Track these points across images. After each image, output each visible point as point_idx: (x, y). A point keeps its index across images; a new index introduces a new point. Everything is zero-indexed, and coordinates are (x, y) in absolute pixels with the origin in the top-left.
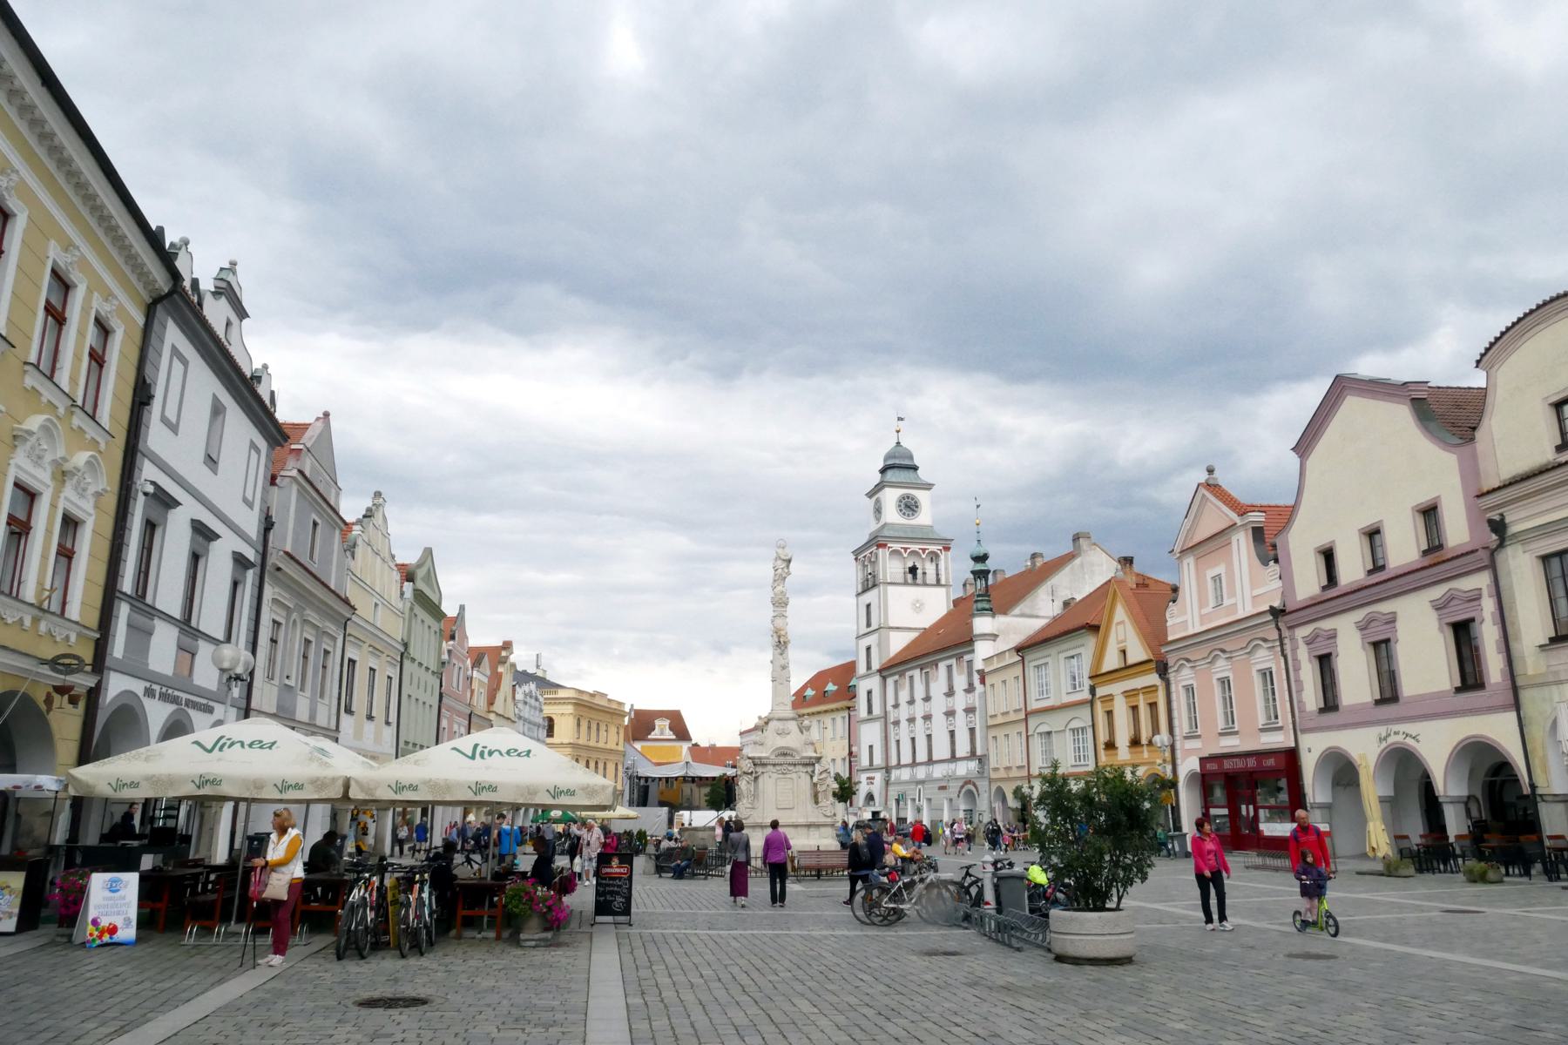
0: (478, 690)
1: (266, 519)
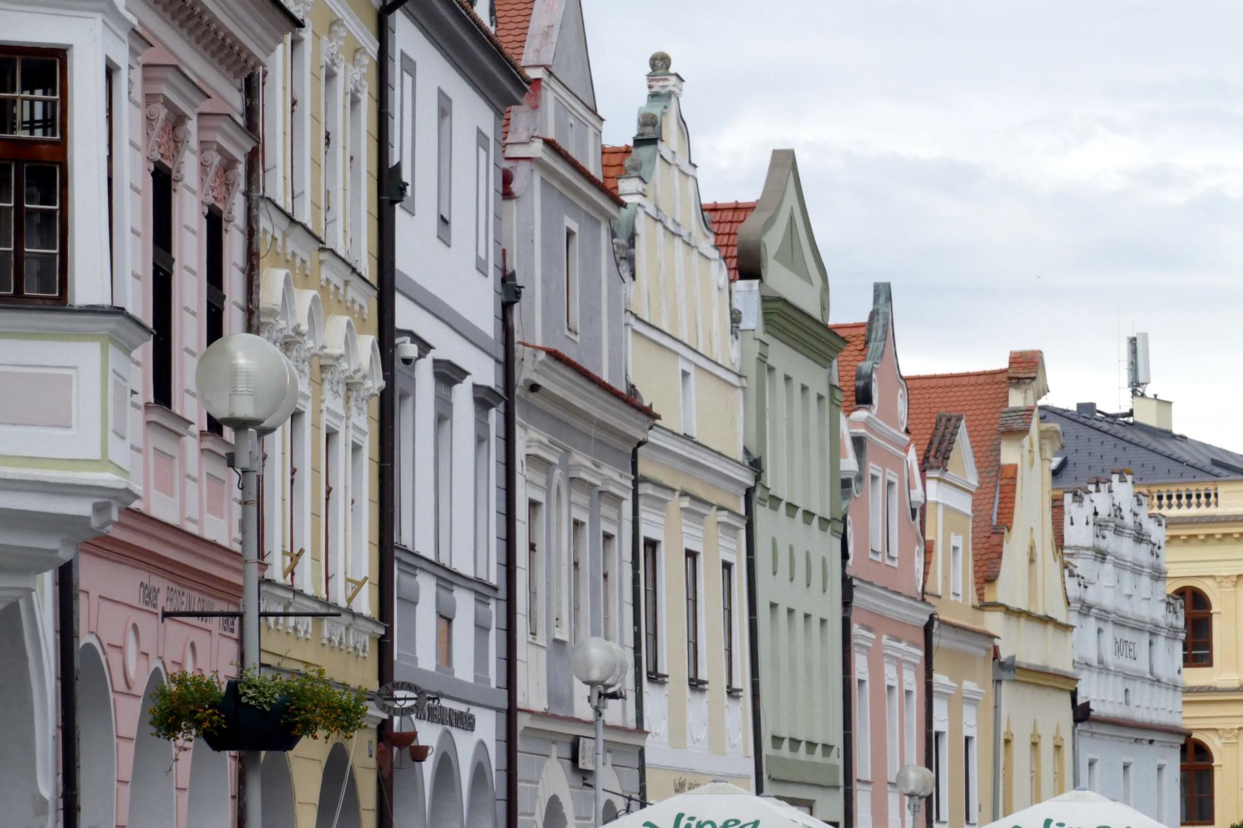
0: (946, 540)
1: (504, 281)
